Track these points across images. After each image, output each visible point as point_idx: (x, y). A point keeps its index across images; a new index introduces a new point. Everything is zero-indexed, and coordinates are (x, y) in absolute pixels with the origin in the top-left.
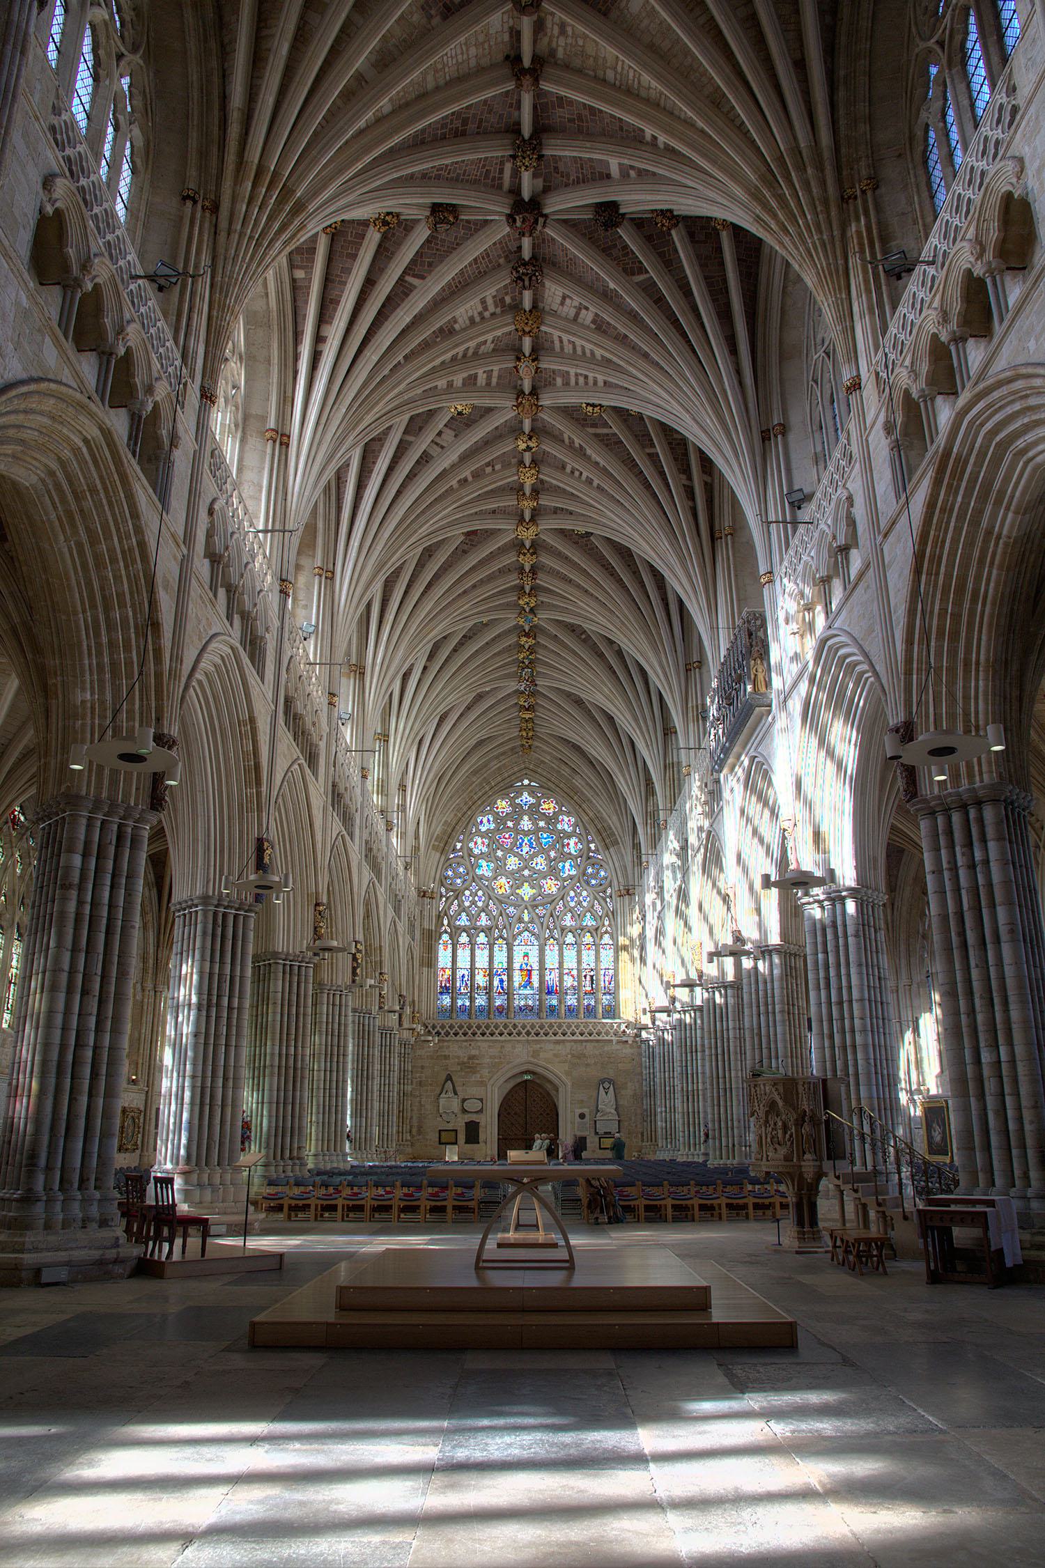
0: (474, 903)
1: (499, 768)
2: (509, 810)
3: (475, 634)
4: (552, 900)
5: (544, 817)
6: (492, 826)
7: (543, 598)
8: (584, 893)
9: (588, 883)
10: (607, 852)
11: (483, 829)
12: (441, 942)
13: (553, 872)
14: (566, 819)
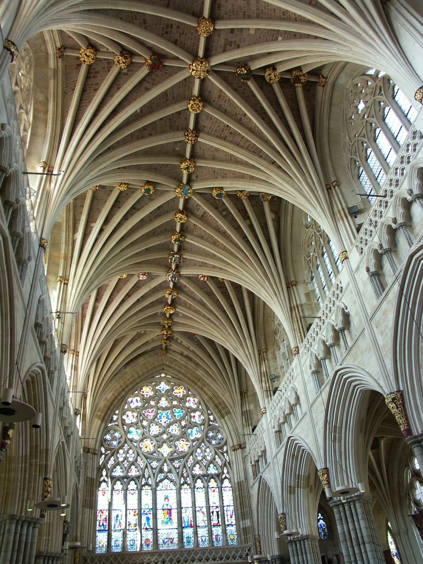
0: (126, 458)
1: (145, 364)
2: (151, 394)
3: (142, 207)
4: (184, 456)
5: (176, 398)
6: (140, 404)
7: (201, 163)
8: (208, 450)
9: (210, 442)
10: (222, 420)
11: (133, 406)
12: (100, 489)
13: (184, 435)
14: (192, 399)
